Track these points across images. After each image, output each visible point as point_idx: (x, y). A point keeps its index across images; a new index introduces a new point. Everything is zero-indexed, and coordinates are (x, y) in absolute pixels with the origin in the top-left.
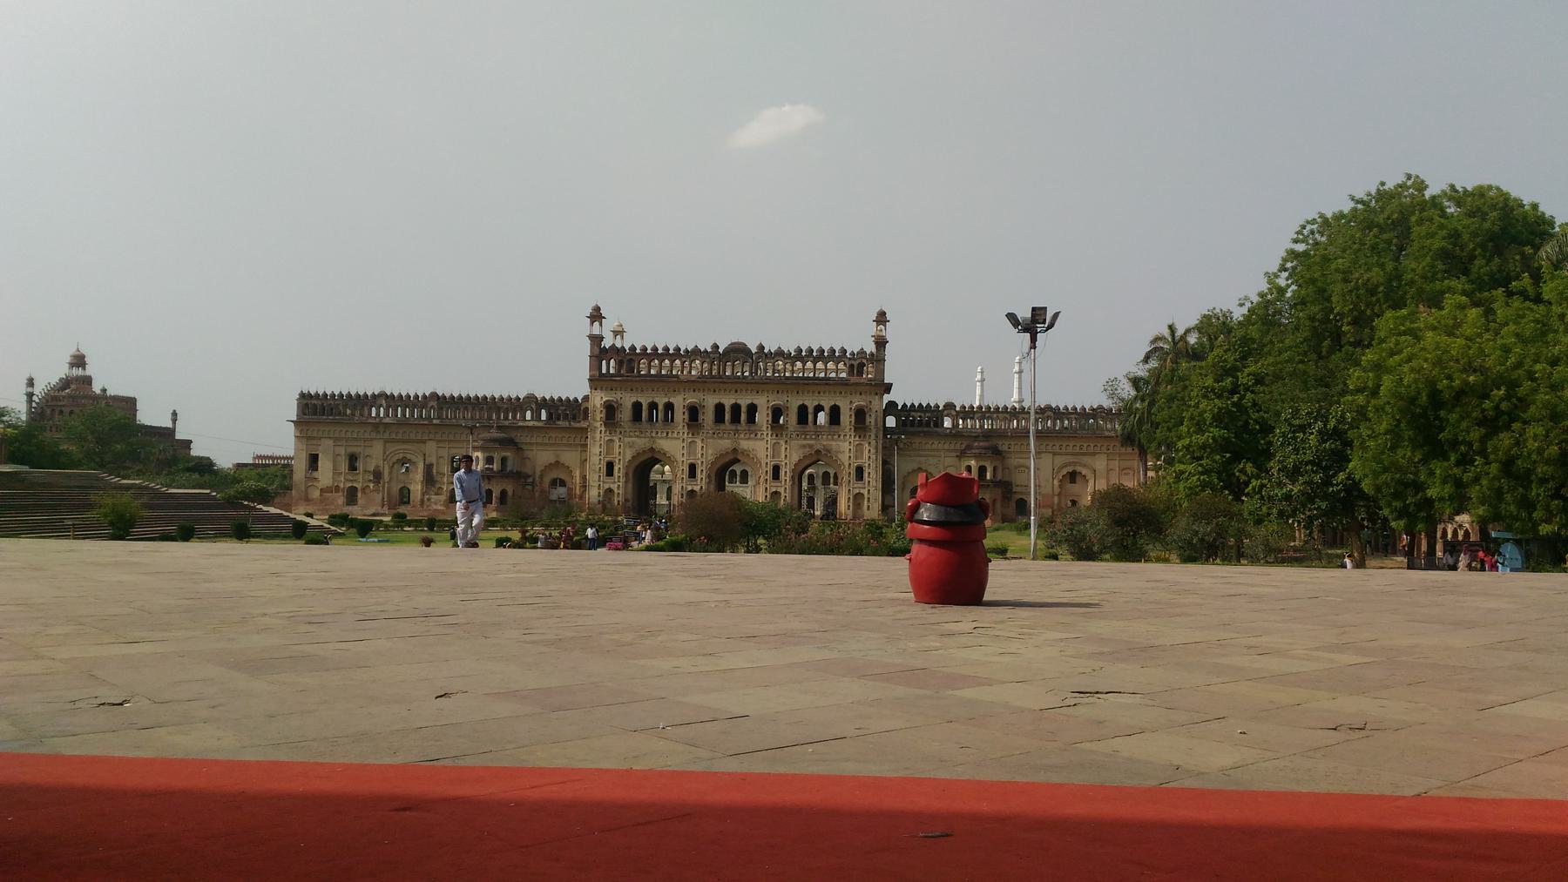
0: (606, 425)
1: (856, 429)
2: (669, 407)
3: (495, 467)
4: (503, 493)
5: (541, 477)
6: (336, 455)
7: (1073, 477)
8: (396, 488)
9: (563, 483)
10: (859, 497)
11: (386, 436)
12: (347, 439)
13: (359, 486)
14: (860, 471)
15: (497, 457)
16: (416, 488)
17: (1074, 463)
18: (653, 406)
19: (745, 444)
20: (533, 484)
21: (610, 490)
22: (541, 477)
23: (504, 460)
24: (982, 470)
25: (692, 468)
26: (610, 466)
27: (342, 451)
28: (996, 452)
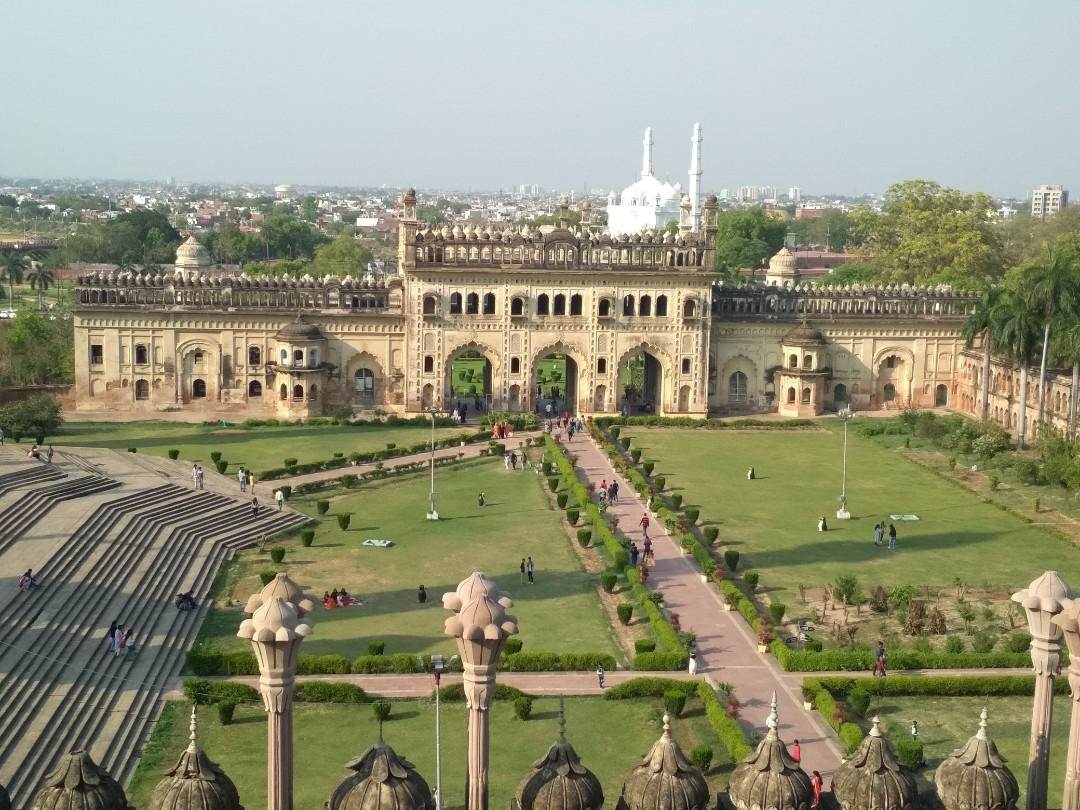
0: (425, 319)
1: (686, 322)
2: (490, 299)
3: (304, 363)
4: (313, 388)
5: (347, 367)
6: (122, 348)
7: (891, 362)
8: (190, 383)
9: (369, 373)
10: (685, 390)
11: (178, 326)
12: (134, 330)
13: (149, 379)
14: (686, 364)
15: (304, 350)
16: (212, 382)
17: (896, 349)
18: (473, 298)
19: (569, 337)
20: (339, 376)
21: (429, 386)
22: (347, 367)
23: (312, 353)
24: (808, 359)
25: (515, 365)
26: (429, 362)
27: (128, 342)
28: (820, 341)
